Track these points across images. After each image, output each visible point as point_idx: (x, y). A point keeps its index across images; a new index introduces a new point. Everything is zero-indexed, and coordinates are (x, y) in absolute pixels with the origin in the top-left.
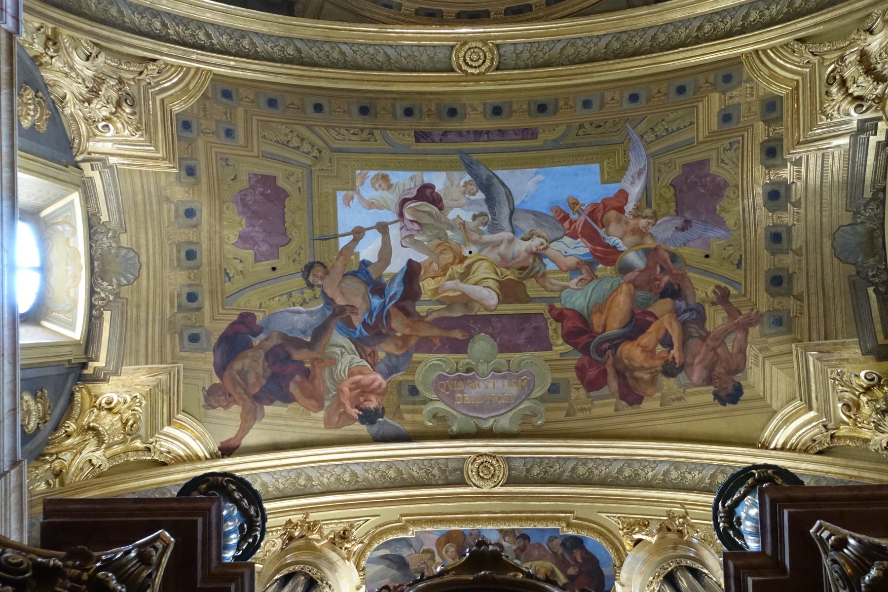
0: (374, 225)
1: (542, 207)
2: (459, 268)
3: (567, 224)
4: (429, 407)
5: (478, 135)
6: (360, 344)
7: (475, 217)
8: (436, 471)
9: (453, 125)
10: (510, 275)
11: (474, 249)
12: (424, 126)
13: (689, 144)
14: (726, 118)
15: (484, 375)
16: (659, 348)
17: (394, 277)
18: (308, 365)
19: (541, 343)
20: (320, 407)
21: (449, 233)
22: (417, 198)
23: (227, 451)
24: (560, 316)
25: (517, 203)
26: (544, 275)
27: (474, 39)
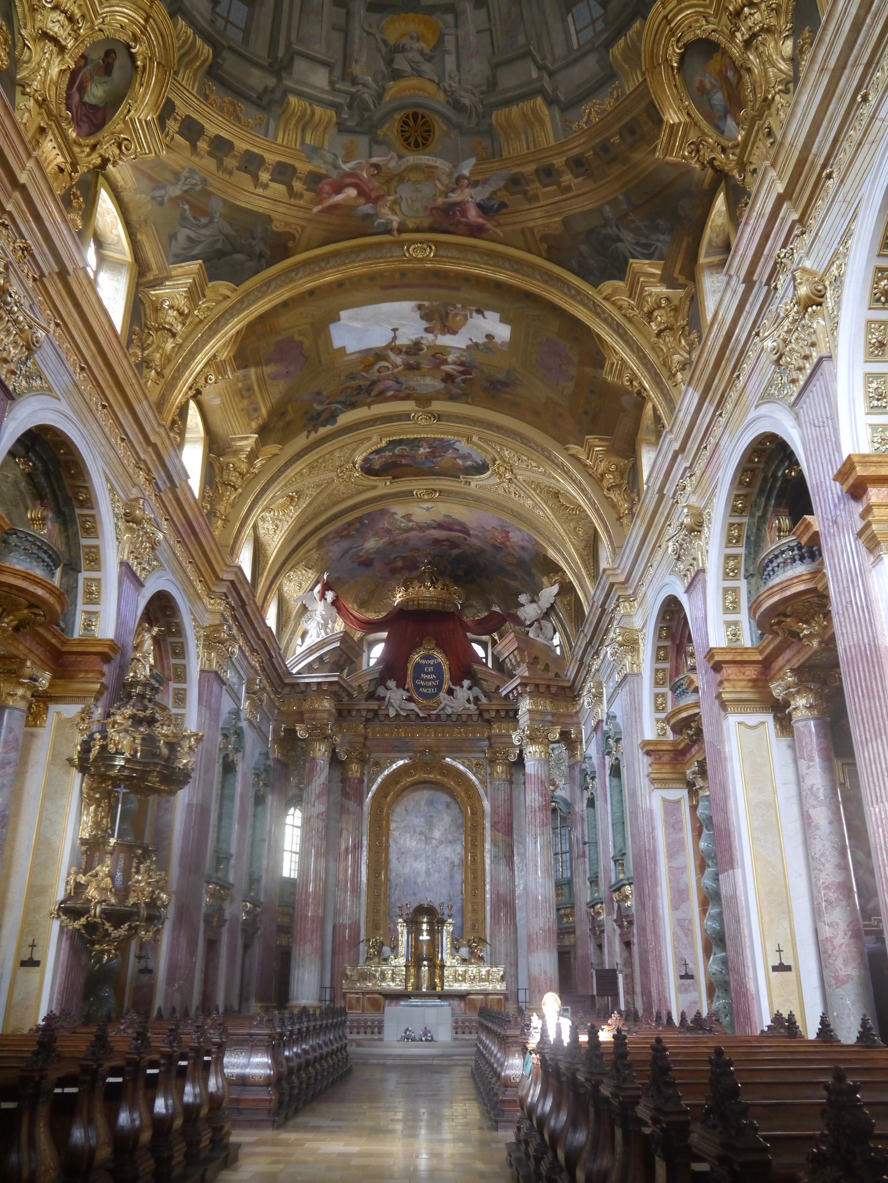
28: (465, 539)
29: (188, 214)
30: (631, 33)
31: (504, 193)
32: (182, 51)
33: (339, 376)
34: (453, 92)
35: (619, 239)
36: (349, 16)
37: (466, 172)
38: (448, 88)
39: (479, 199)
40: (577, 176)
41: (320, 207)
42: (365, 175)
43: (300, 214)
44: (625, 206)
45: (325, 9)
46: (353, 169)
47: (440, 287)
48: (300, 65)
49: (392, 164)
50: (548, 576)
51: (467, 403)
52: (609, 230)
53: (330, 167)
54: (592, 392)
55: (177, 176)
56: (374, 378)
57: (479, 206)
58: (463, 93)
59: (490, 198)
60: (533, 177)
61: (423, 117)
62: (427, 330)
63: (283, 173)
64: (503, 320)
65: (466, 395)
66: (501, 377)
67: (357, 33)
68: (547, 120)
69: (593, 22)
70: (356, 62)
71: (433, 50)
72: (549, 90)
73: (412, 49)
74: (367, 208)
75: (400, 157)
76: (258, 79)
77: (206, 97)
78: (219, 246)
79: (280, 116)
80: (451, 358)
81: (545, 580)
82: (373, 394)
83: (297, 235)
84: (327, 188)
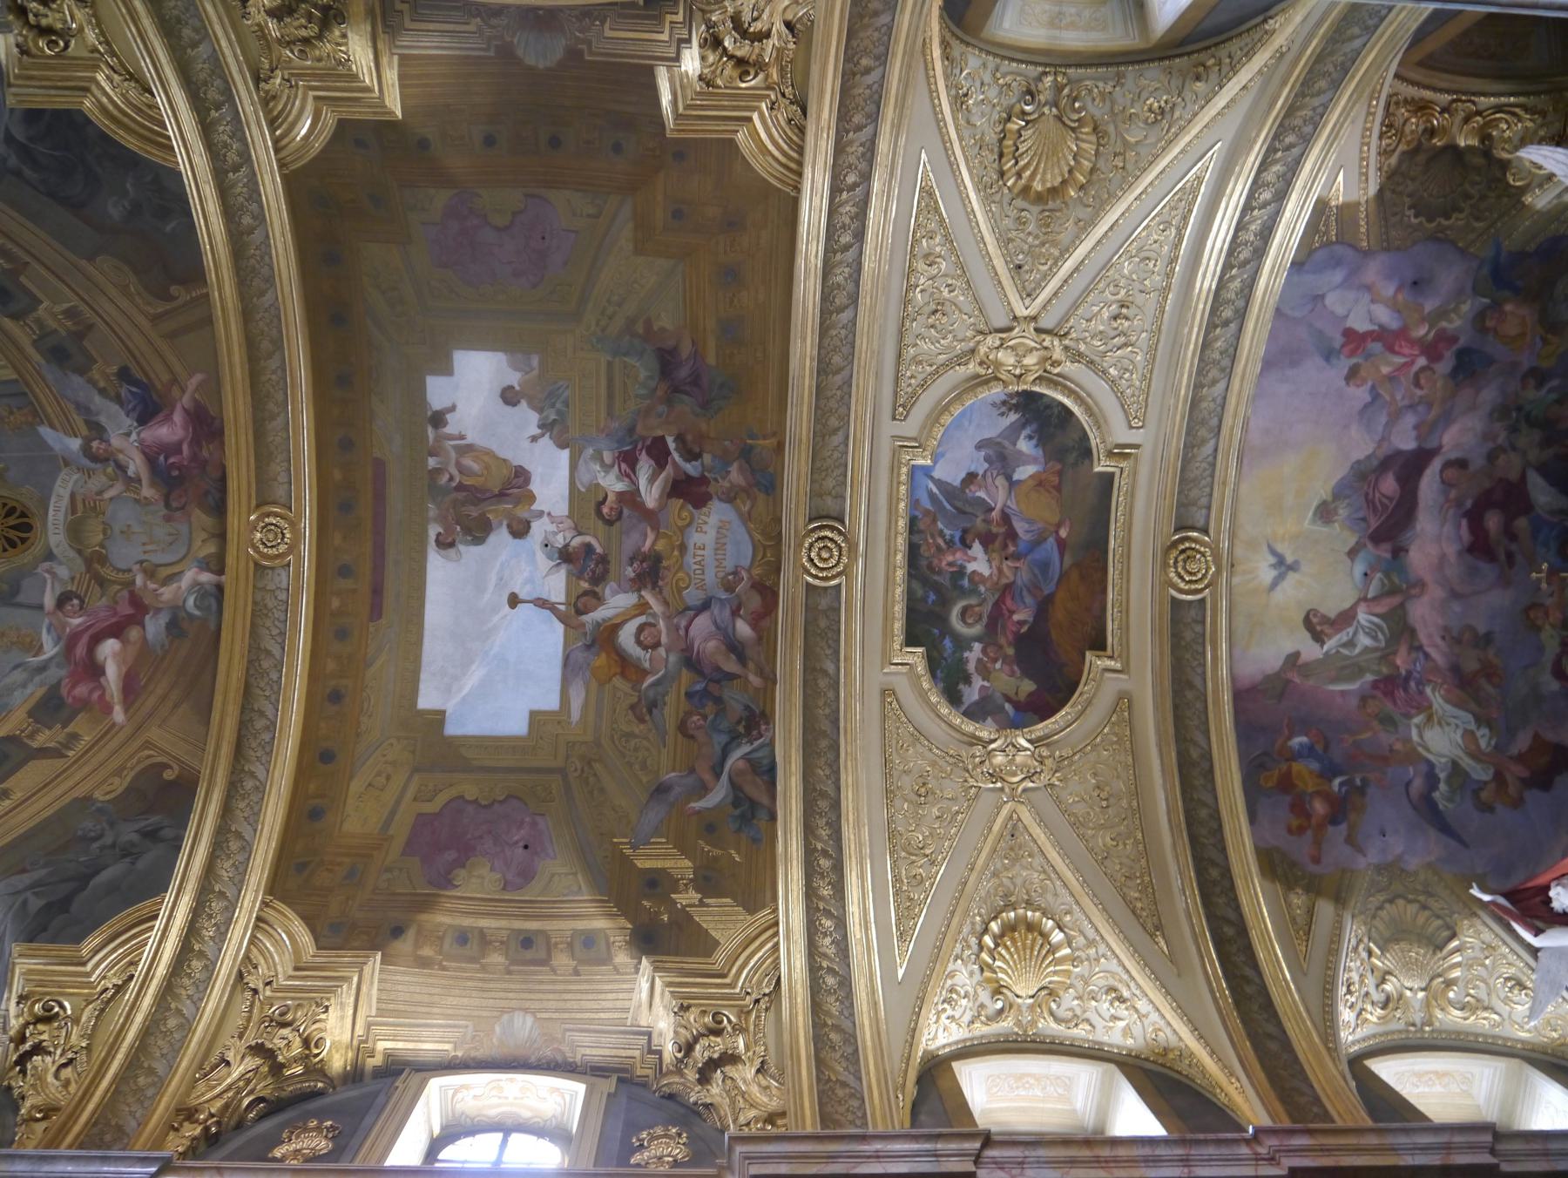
28: (1462, 464)
33: (629, 736)
37: (75, 444)
39: (128, 422)
42: (77, 621)
47: (380, 497)
49: (63, 572)
50: (1523, 190)
51: (780, 447)
53: (37, 679)
54: (555, 142)
56: (673, 658)
57: (143, 420)
59: (118, 400)
62: (520, 530)
64: (447, 370)
65: (746, 454)
66: (643, 369)
74: (154, 627)
75: (49, 556)
78: (36, 904)
80: (613, 484)
81: (1540, 200)
82: (731, 666)
83: (159, 759)
84: (81, 690)
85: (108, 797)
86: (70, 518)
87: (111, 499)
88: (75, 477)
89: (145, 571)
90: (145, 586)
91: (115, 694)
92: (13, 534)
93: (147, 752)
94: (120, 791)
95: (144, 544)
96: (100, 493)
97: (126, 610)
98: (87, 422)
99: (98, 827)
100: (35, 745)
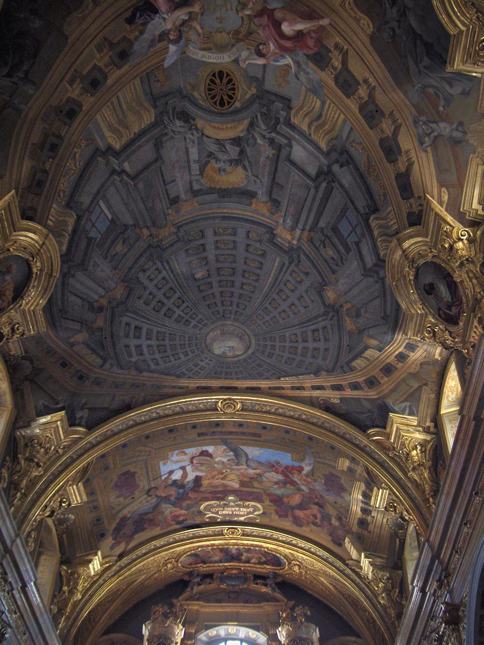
0: (179, 467)
1: (263, 460)
2: (221, 476)
3: (274, 469)
4: (207, 516)
5: (231, 433)
6: (174, 504)
7: (228, 460)
8: (211, 532)
9: (218, 429)
10: (246, 479)
11: (228, 471)
12: (204, 430)
13: (334, 468)
14: (350, 470)
15: (232, 506)
16: (311, 517)
17: (189, 482)
18: (151, 518)
19: (258, 499)
20: (158, 525)
21: (216, 465)
22: (199, 456)
23: (121, 556)
24: (269, 495)
25: (250, 457)
26: (262, 482)
27: (230, 399)
29: (442, 102)
30: (66, 240)
31: (132, 37)
32: (388, 238)
34: (191, 129)
35: (9, 75)
36: (270, 193)
37: (172, 48)
38: (195, 132)
39: (157, 19)
40: (68, 101)
41: (321, 22)
42: (272, 46)
43: (342, 25)
44: (16, 101)
45: (286, 200)
46: (283, 57)
48: (312, 170)
49: (244, 54)
52: (21, 75)
53: (304, 67)
55: (434, 145)
57: (155, 11)
58: (182, 130)
59: (145, 24)
60: (106, 70)
61: (215, 103)
63: (347, 84)
67: (266, 180)
68: (108, 134)
69: (93, 225)
70: (268, 158)
71: (209, 162)
72: (112, 160)
73: (224, 162)
75: (236, 61)
76: (345, 177)
77: (385, 195)
78: (426, 61)
79: (336, 138)
84: (311, 43)
85: (371, 26)
86: (214, 51)
87: (202, 28)
88: (191, 48)
89: (243, 9)
90: (251, 9)
91: (313, 24)
92: (225, 81)
93: (347, 5)
94: (367, 19)
95: (227, 10)
96: (199, 35)
97: (265, 20)
98: (159, 41)
99: (387, 30)
100: (340, 66)
